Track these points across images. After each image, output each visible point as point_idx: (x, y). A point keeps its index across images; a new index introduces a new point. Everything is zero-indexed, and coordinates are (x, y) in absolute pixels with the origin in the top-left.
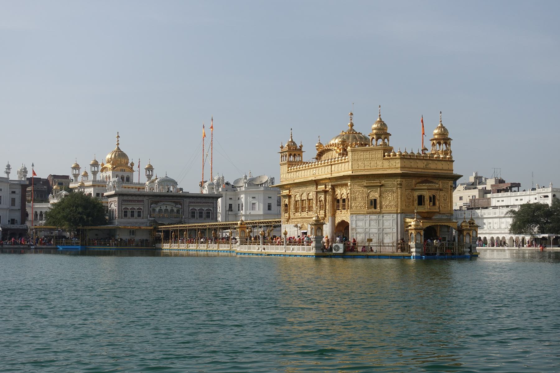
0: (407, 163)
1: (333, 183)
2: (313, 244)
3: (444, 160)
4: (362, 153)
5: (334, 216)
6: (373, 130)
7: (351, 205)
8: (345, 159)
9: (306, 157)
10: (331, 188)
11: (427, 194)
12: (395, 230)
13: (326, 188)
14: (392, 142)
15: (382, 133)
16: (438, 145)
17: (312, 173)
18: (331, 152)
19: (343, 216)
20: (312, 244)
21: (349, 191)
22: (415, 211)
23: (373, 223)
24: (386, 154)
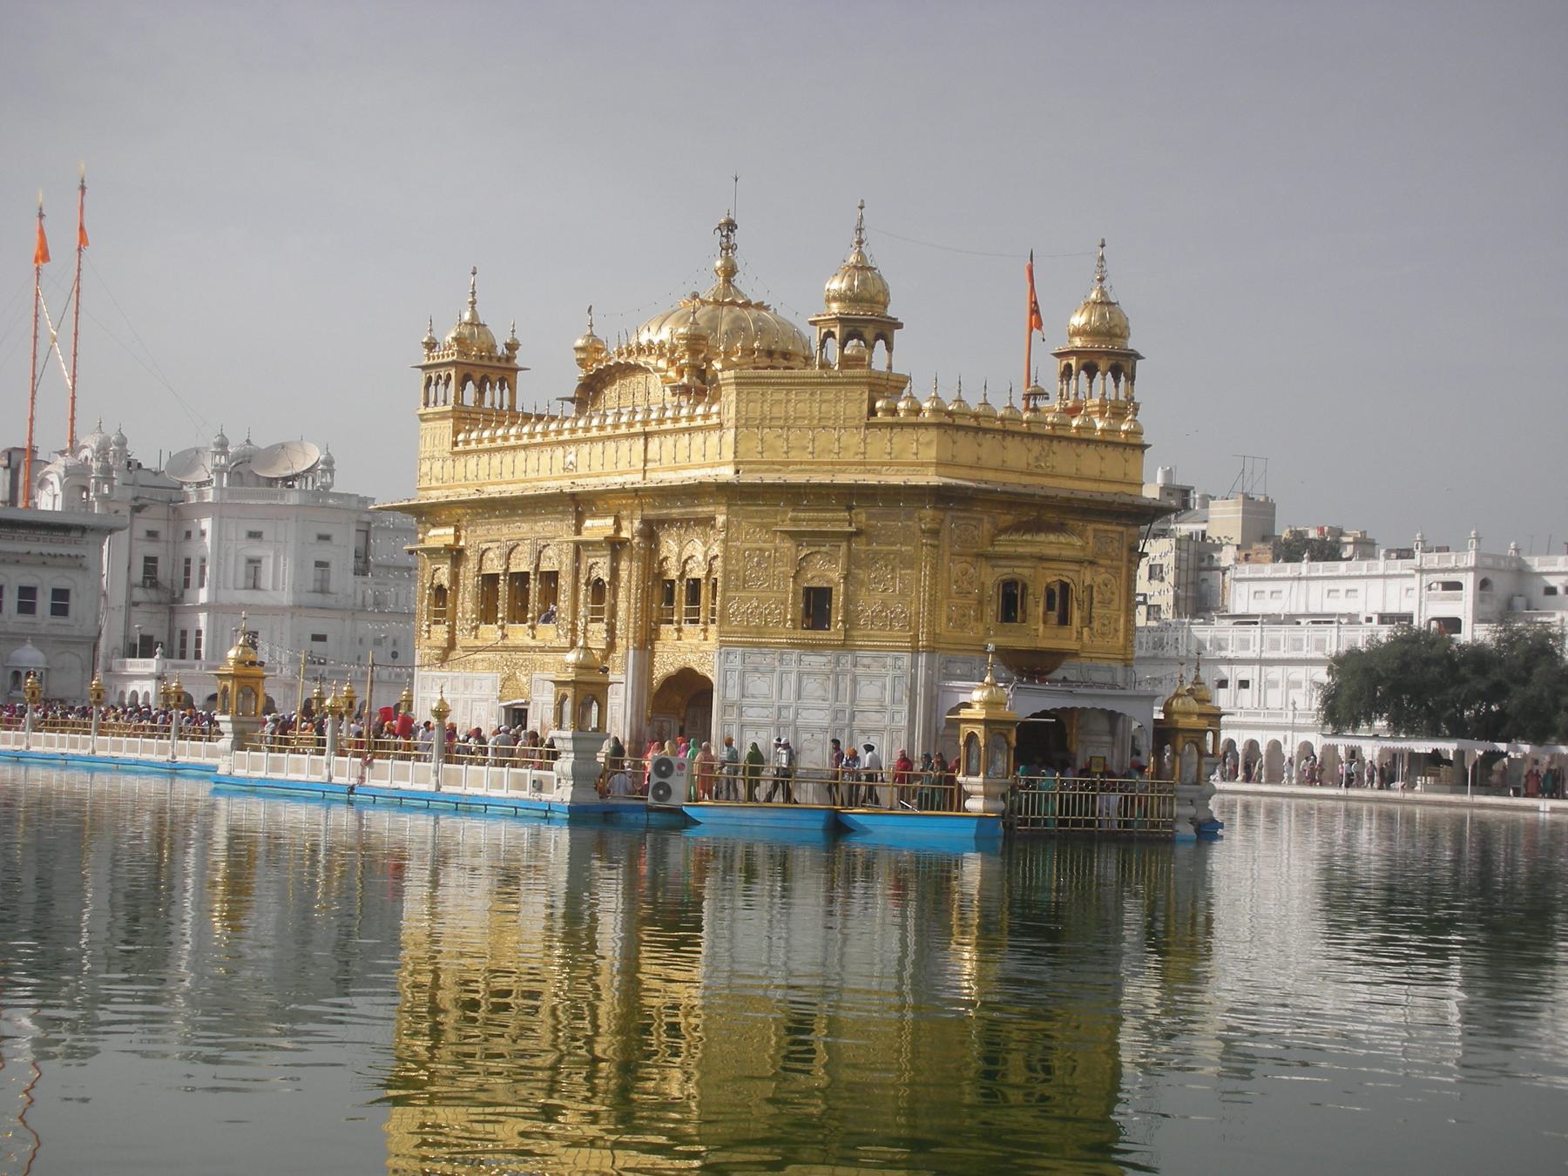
0: (966, 448)
1: (651, 513)
2: (565, 764)
3: (1108, 442)
4: (781, 396)
5: (647, 642)
6: (828, 300)
7: (723, 608)
8: (706, 416)
9: (531, 391)
10: (641, 533)
13: (618, 529)
15: (867, 320)
17: (558, 464)
18: (640, 377)
19: (687, 647)
20: (557, 764)
21: (716, 550)
22: (991, 647)
23: (811, 686)
24: (879, 404)
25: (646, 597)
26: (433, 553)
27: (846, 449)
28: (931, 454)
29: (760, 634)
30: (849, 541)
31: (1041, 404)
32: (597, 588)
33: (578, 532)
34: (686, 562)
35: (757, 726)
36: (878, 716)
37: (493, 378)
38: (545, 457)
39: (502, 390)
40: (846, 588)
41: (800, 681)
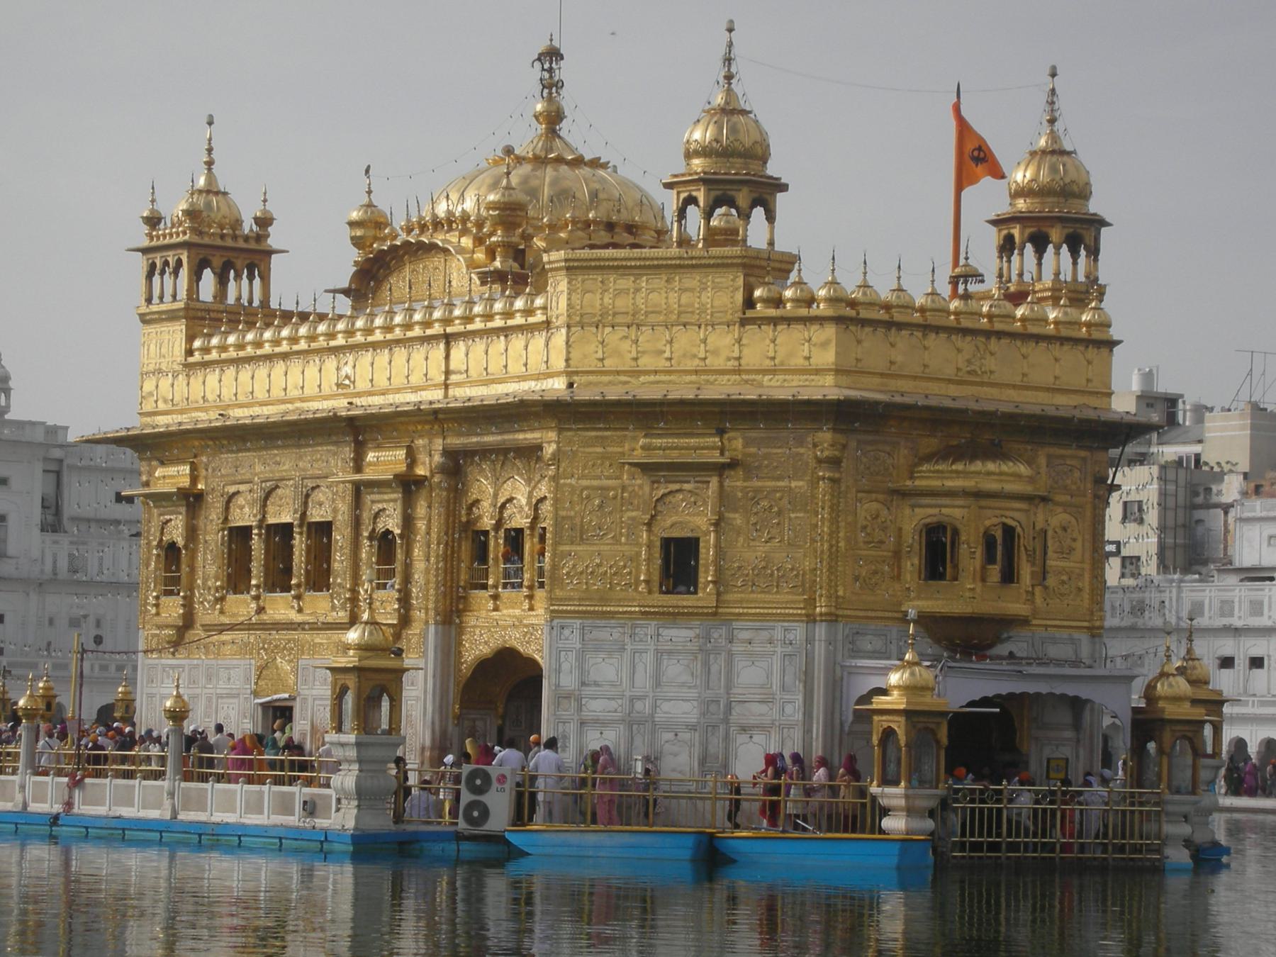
1: (456, 441)
2: (346, 779)
5: (452, 614)
6: (689, 155)
7: (555, 567)
8: (528, 312)
10: (443, 469)
11: (971, 524)
12: (794, 711)
14: (791, 227)
16: (1029, 248)
17: (330, 377)
19: (507, 620)
20: (336, 780)
21: (543, 489)
22: (912, 613)
24: (758, 293)
25: (450, 557)
26: (160, 499)
27: (716, 353)
28: (828, 357)
29: (604, 600)
30: (721, 476)
31: (973, 288)
32: (385, 542)
33: (358, 468)
34: (503, 506)
35: (601, 723)
36: (763, 708)
37: (239, 263)
38: (312, 371)
39: (251, 278)
40: (718, 539)
41: (658, 663)
